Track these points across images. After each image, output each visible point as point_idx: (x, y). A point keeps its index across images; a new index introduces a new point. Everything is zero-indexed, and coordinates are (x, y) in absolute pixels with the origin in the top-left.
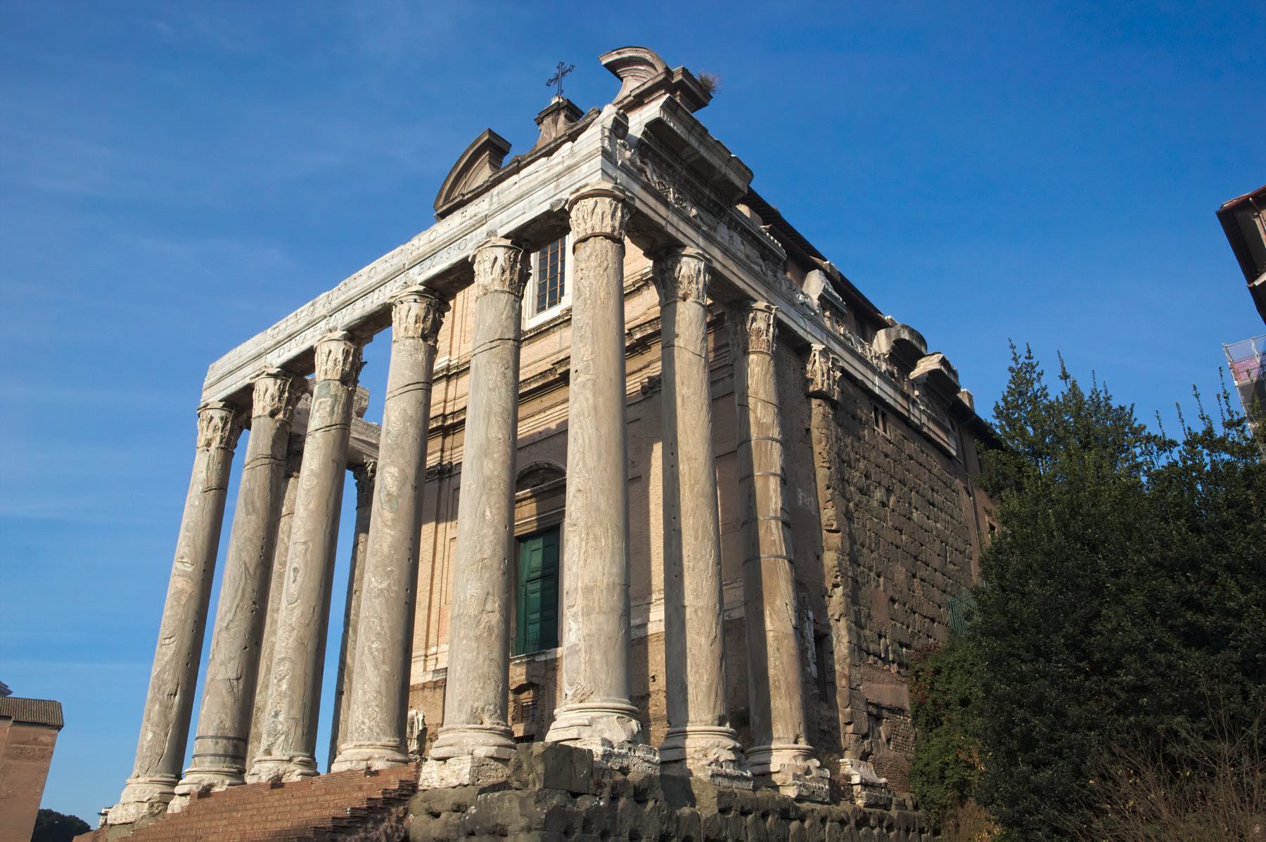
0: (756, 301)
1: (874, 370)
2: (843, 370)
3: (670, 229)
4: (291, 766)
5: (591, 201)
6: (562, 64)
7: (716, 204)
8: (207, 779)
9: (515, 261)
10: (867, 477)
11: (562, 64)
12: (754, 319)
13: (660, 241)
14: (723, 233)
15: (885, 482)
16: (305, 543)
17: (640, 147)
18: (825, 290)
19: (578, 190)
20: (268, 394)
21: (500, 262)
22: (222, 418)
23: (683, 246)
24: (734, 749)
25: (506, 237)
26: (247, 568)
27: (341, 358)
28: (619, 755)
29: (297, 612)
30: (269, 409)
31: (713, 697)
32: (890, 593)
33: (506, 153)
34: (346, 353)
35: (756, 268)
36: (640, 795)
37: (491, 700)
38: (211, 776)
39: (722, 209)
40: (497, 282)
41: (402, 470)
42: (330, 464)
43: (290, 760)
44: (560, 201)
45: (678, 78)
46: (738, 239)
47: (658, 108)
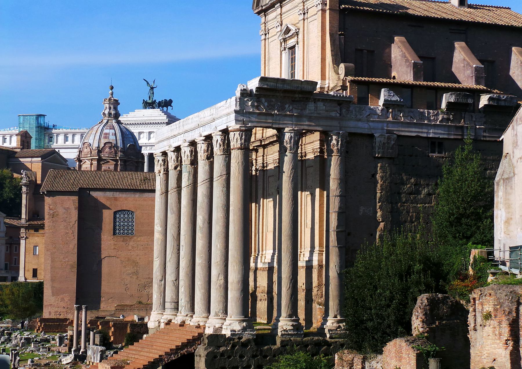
4: (187, 318)
7: (303, 98)
8: (170, 317)
9: (225, 140)
14: (311, 106)
16: (184, 235)
20: (172, 159)
21: (219, 141)
22: (163, 160)
24: (292, 325)
26: (174, 237)
27: (189, 154)
28: (238, 334)
29: (184, 262)
30: (173, 166)
31: (287, 308)
35: (333, 114)
36: (245, 345)
37: (222, 309)
38: (170, 316)
39: (307, 98)
40: (218, 150)
41: (203, 217)
42: (190, 202)
43: (187, 316)
46: (320, 105)
47: (258, 82)
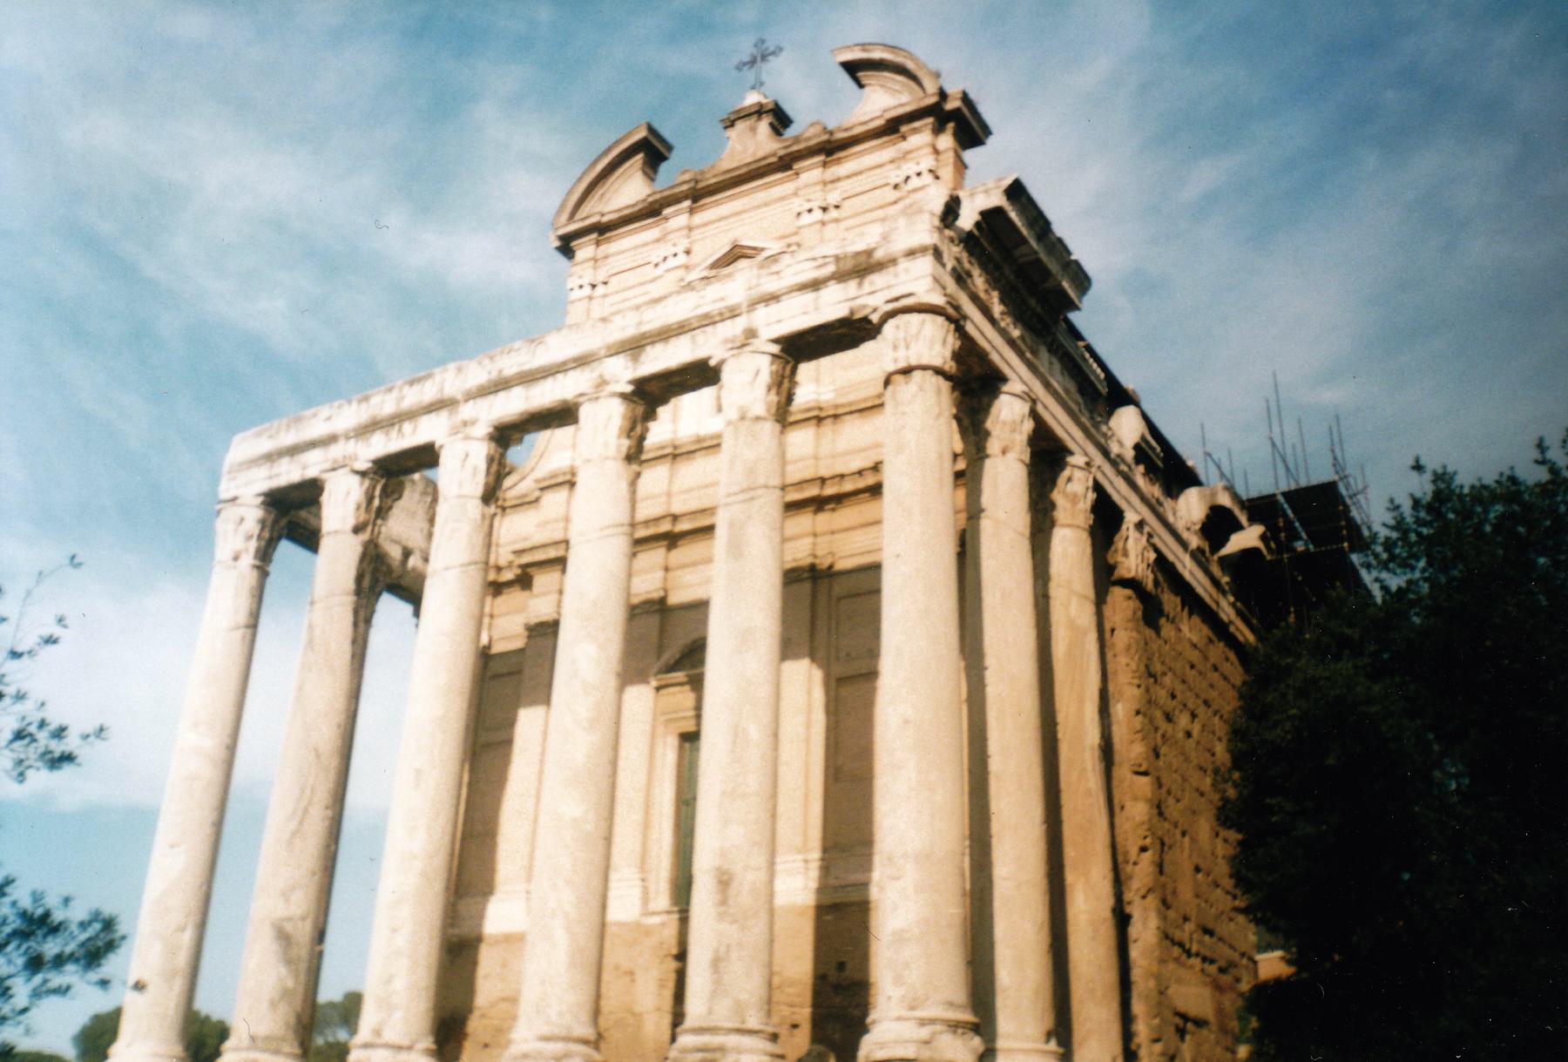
0: (1072, 453)
1: (1184, 544)
2: (1156, 550)
3: (995, 357)
5: (915, 318)
6: (763, 41)
10: (1173, 697)
11: (763, 41)
12: (1069, 480)
13: (977, 370)
15: (1190, 705)
17: (969, 241)
18: (1143, 438)
19: (897, 299)
23: (1004, 379)
25: (776, 341)
26: (318, 756)
32: (1196, 860)
33: (663, 158)
34: (490, 460)
44: (865, 307)
45: (951, 105)
